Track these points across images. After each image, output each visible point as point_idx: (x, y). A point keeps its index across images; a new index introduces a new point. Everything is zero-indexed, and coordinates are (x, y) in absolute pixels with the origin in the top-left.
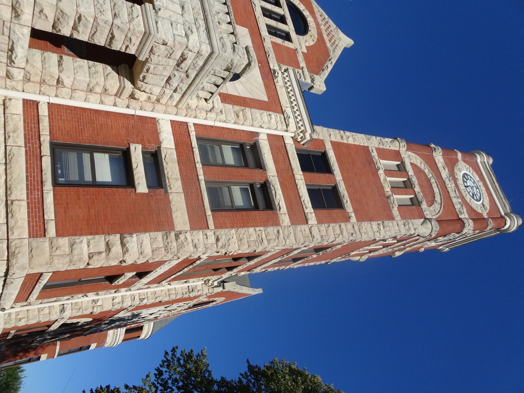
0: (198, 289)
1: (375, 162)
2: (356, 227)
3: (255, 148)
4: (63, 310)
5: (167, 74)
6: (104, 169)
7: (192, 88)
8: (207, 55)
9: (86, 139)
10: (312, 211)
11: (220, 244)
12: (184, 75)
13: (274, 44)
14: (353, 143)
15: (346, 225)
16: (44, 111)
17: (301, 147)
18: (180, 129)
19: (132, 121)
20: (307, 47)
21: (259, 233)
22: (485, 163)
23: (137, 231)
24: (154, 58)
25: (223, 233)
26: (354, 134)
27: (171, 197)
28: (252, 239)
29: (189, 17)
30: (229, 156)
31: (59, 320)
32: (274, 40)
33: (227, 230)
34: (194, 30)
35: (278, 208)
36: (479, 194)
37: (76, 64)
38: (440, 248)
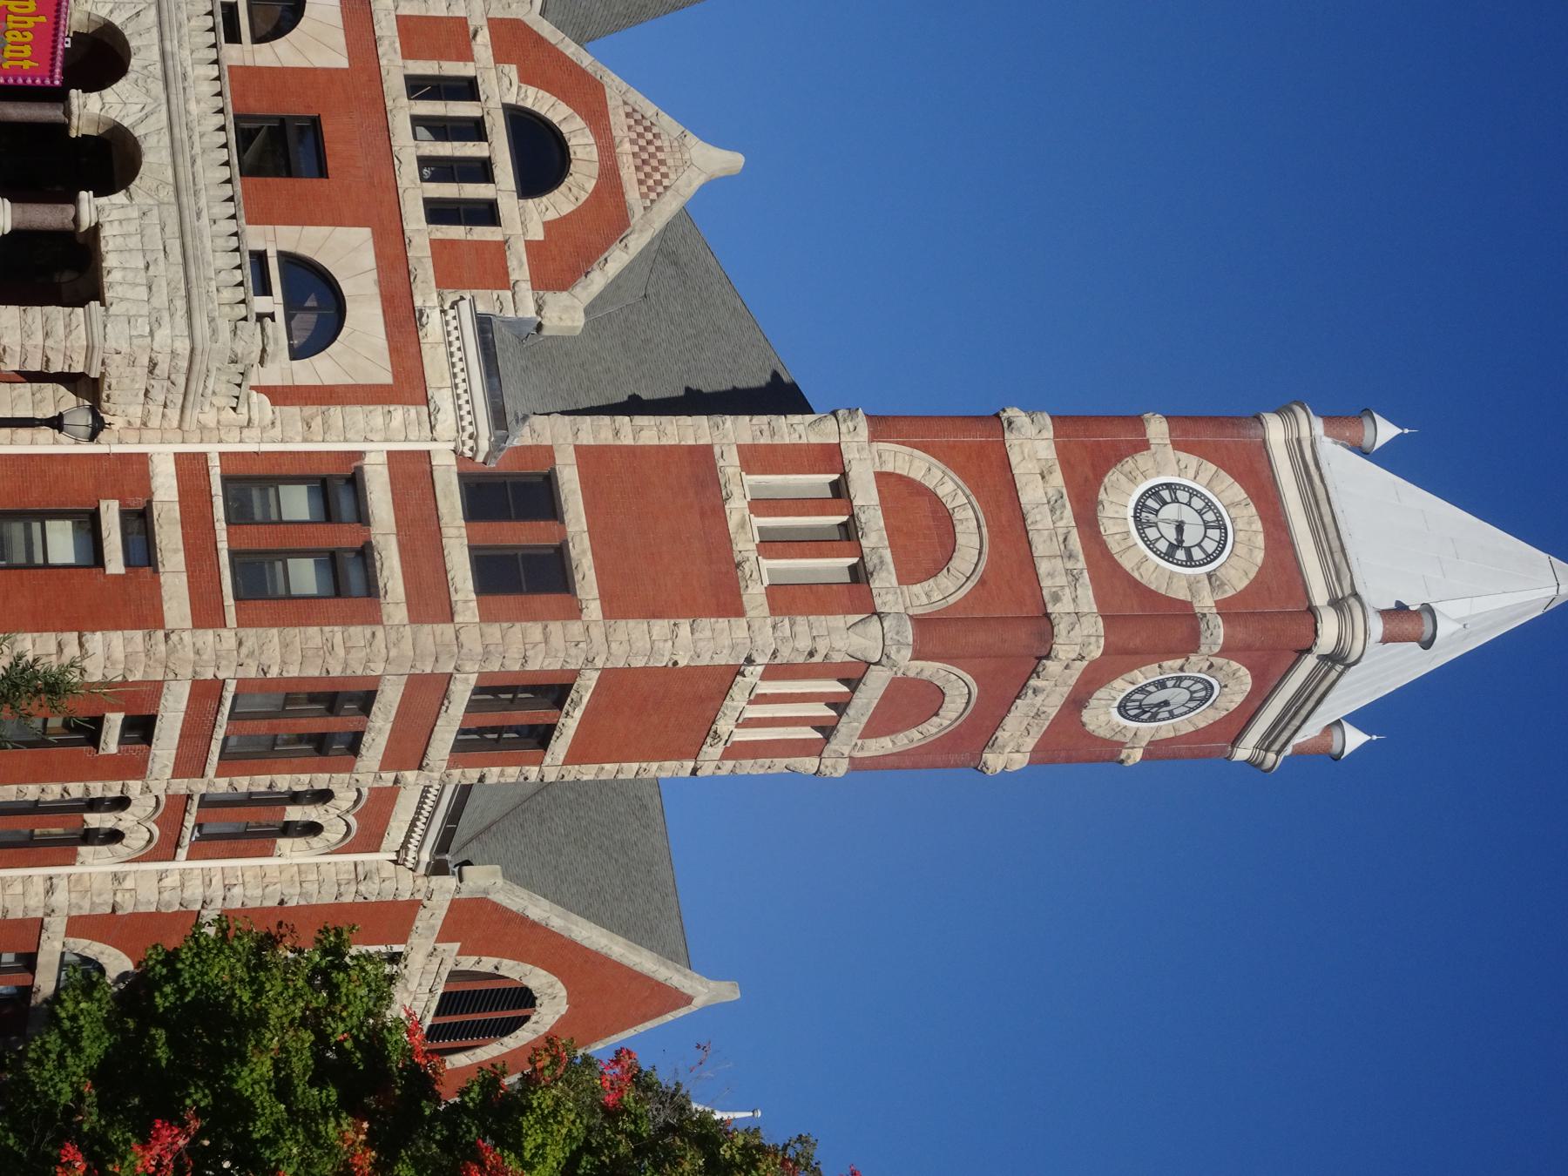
0: (384, 875)
1: (722, 482)
2: (597, 633)
3: (355, 482)
4: (50, 890)
5: (141, 385)
6: (61, 543)
7: (191, 398)
8: (187, 352)
9: (33, 501)
10: (473, 596)
11: (244, 650)
12: (167, 383)
13: (438, 247)
14: (656, 442)
15: (564, 627)
17: (471, 468)
18: (191, 468)
19: (105, 464)
20: (548, 226)
21: (329, 635)
22: (1299, 441)
23: (102, 628)
24: (112, 371)
25: (251, 635)
26: (664, 419)
27: (162, 579)
28: (310, 645)
29: (160, 299)
30: (297, 503)
31: (46, 920)
32: (439, 235)
33: (260, 630)
34: (166, 315)
35: (382, 593)
36: (1210, 546)
37: (15, 393)
38: (1243, 753)
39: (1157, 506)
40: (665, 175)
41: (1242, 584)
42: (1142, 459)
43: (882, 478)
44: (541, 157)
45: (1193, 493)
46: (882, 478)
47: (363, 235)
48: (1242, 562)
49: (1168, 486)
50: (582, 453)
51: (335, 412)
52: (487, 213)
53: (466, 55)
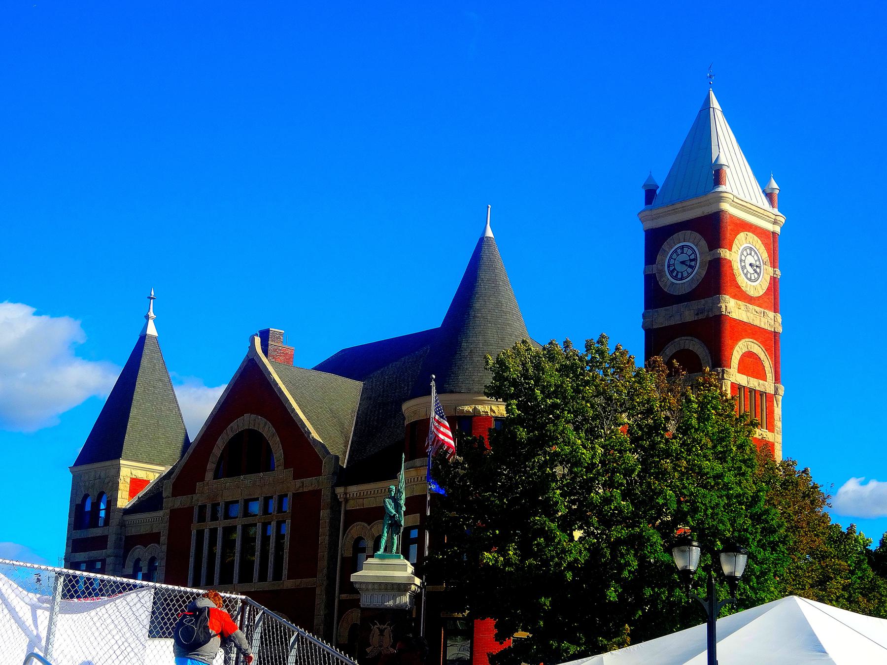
45: (671, 257)
49: (669, 267)
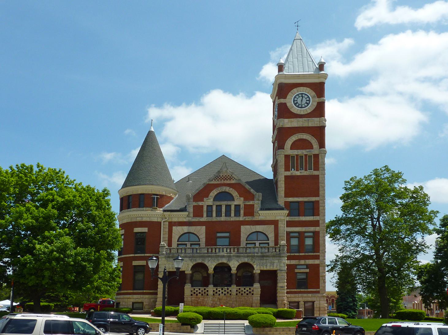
16: (288, 290)
36: (306, 97)
39: (298, 104)
40: (229, 176)
41: (314, 93)
42: (288, 105)
43: (292, 148)
44: (223, 196)
46: (292, 148)
47: (243, 228)
48: (310, 93)
50: (286, 196)
51: (280, 235)
52: (237, 207)
53: (202, 206)
